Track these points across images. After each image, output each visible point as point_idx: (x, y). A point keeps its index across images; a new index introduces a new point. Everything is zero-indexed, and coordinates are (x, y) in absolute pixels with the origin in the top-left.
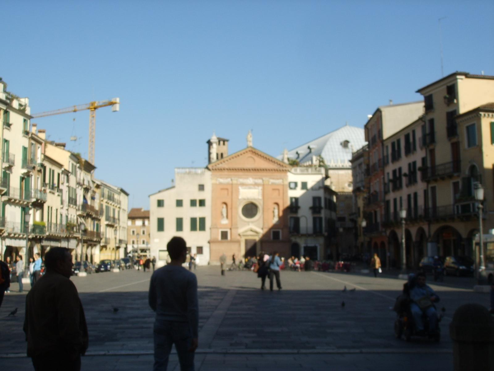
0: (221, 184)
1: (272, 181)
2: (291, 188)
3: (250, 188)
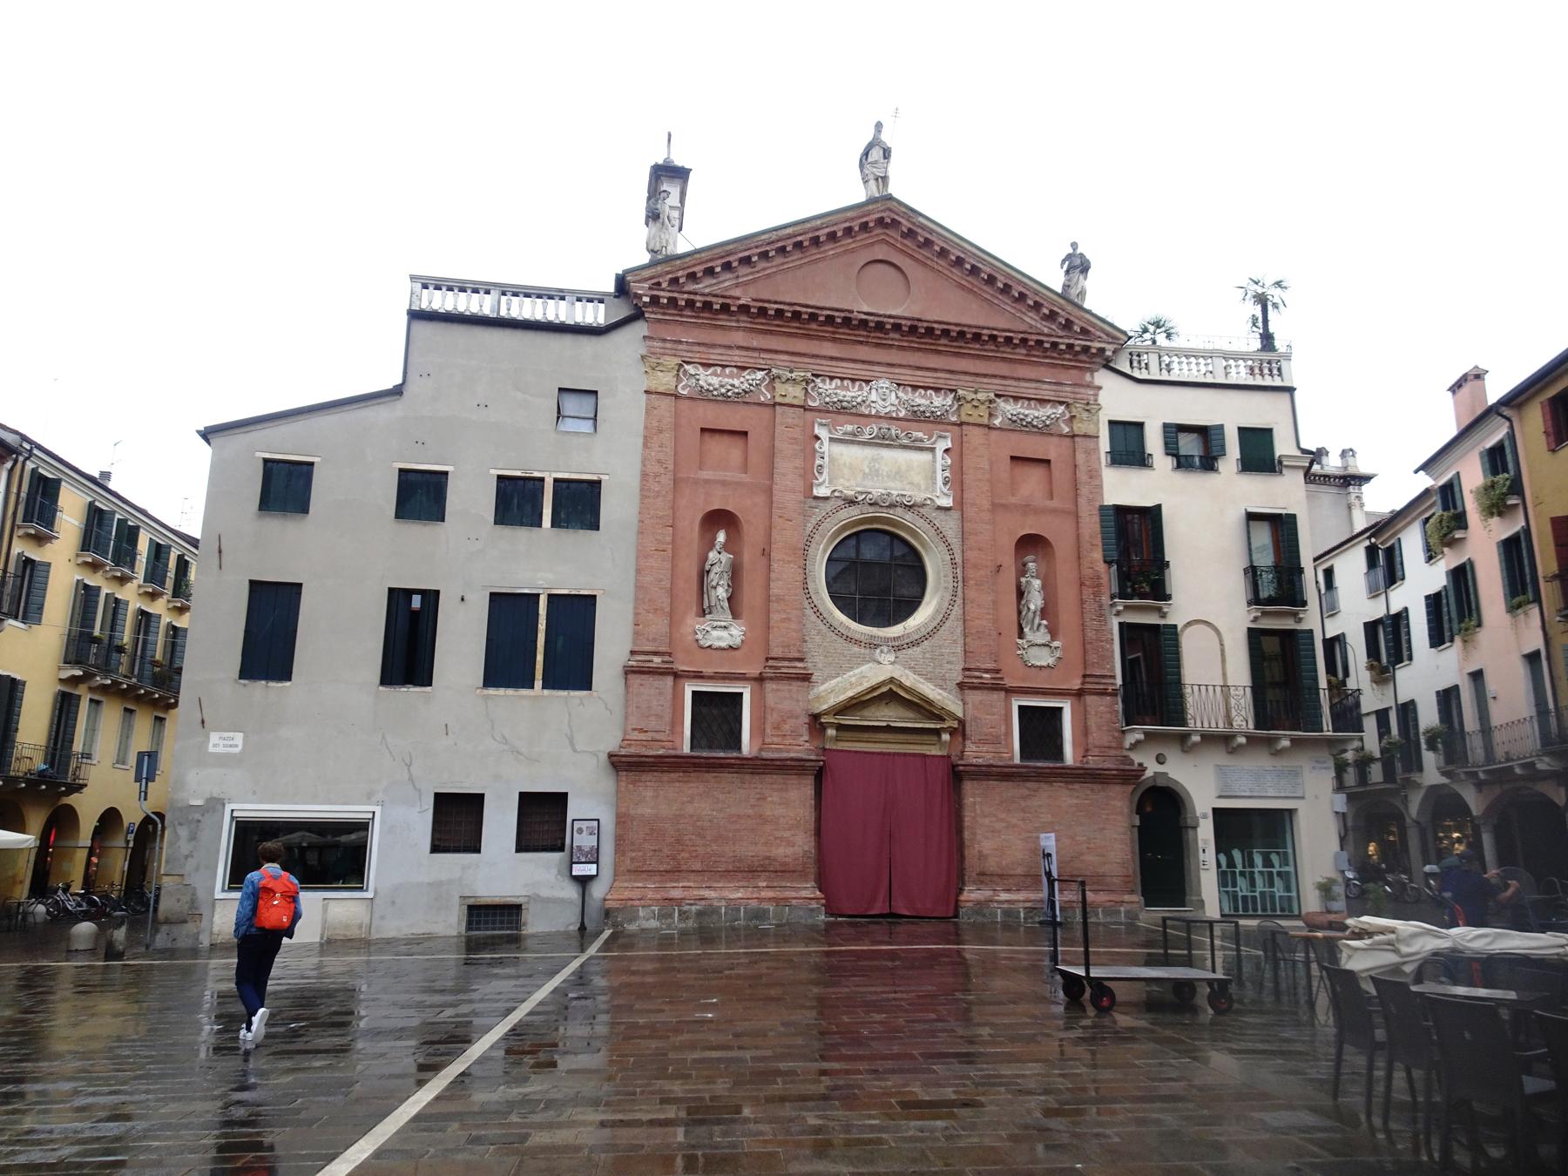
1: (1009, 408)
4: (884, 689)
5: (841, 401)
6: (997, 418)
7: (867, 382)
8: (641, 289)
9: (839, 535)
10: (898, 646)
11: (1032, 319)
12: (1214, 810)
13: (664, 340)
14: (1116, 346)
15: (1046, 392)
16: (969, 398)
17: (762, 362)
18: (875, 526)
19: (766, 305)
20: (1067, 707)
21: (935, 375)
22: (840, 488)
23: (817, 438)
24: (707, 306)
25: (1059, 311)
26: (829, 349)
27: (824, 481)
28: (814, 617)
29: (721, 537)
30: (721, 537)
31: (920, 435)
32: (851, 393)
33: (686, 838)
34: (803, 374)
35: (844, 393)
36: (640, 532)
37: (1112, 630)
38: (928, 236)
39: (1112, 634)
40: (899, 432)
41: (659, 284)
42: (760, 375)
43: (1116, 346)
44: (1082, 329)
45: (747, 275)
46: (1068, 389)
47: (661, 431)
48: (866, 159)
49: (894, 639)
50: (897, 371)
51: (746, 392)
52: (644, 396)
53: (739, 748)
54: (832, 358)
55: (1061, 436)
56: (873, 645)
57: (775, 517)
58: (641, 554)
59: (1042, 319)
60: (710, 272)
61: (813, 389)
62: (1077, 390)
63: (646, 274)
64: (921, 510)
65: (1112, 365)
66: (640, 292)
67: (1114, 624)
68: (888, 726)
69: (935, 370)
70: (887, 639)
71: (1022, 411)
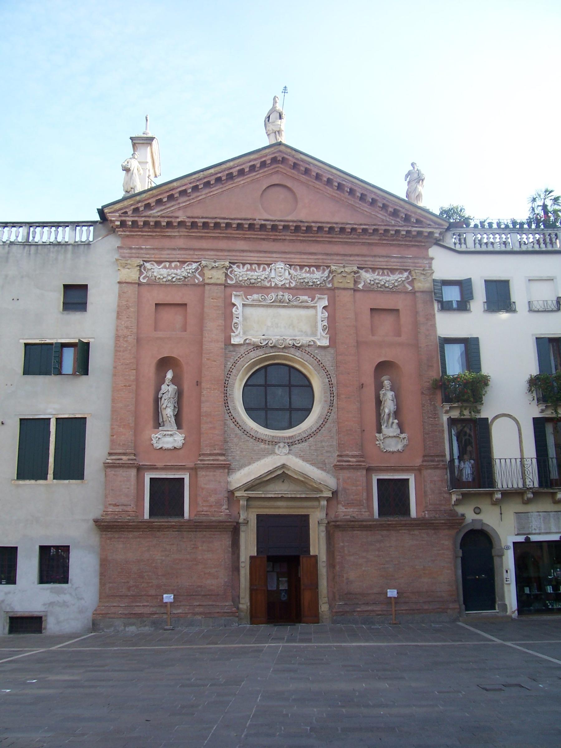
0: (154, 283)
1: (367, 276)
2: (446, 307)
3: (280, 304)
4: (279, 472)
5: (250, 279)
6: (360, 283)
7: (269, 265)
8: (114, 217)
9: (251, 369)
10: (291, 443)
11: (382, 215)
12: (514, 543)
13: (131, 248)
14: (442, 230)
15: (394, 264)
16: (339, 271)
17: (195, 257)
18: (276, 361)
19: (196, 220)
20: (412, 478)
21: (316, 257)
22: (249, 337)
23: (234, 305)
24: (157, 224)
25: (401, 209)
26: (241, 245)
27: (239, 333)
28: (232, 425)
29: (169, 375)
30: (169, 375)
31: (306, 298)
32: (259, 274)
33: (145, 574)
34: (223, 263)
35: (252, 273)
36: (114, 375)
37: (443, 424)
38: (308, 166)
39: (443, 427)
40: (291, 297)
41: (126, 213)
42: (194, 266)
43: (442, 230)
44: (417, 220)
45: (184, 202)
46: (410, 261)
47: (128, 308)
48: (269, 121)
49: (290, 438)
50: (288, 256)
51: (185, 278)
52: (118, 285)
53: (183, 515)
54: (243, 251)
55: (406, 293)
56: (274, 442)
57: (204, 360)
58: (115, 389)
59: (390, 215)
60: (159, 202)
61: (231, 272)
62: (416, 261)
63: (117, 206)
64: (307, 349)
65: (442, 243)
66: (113, 219)
67: (445, 418)
68: (282, 497)
69: (315, 254)
70: (284, 438)
71: (378, 277)
